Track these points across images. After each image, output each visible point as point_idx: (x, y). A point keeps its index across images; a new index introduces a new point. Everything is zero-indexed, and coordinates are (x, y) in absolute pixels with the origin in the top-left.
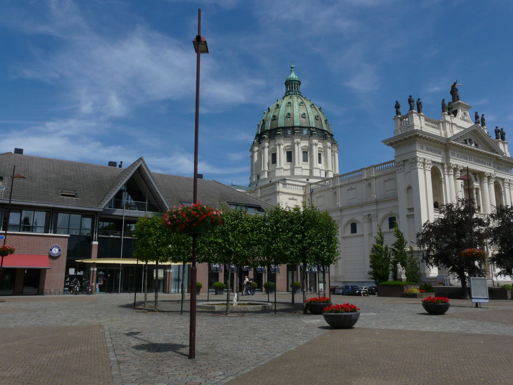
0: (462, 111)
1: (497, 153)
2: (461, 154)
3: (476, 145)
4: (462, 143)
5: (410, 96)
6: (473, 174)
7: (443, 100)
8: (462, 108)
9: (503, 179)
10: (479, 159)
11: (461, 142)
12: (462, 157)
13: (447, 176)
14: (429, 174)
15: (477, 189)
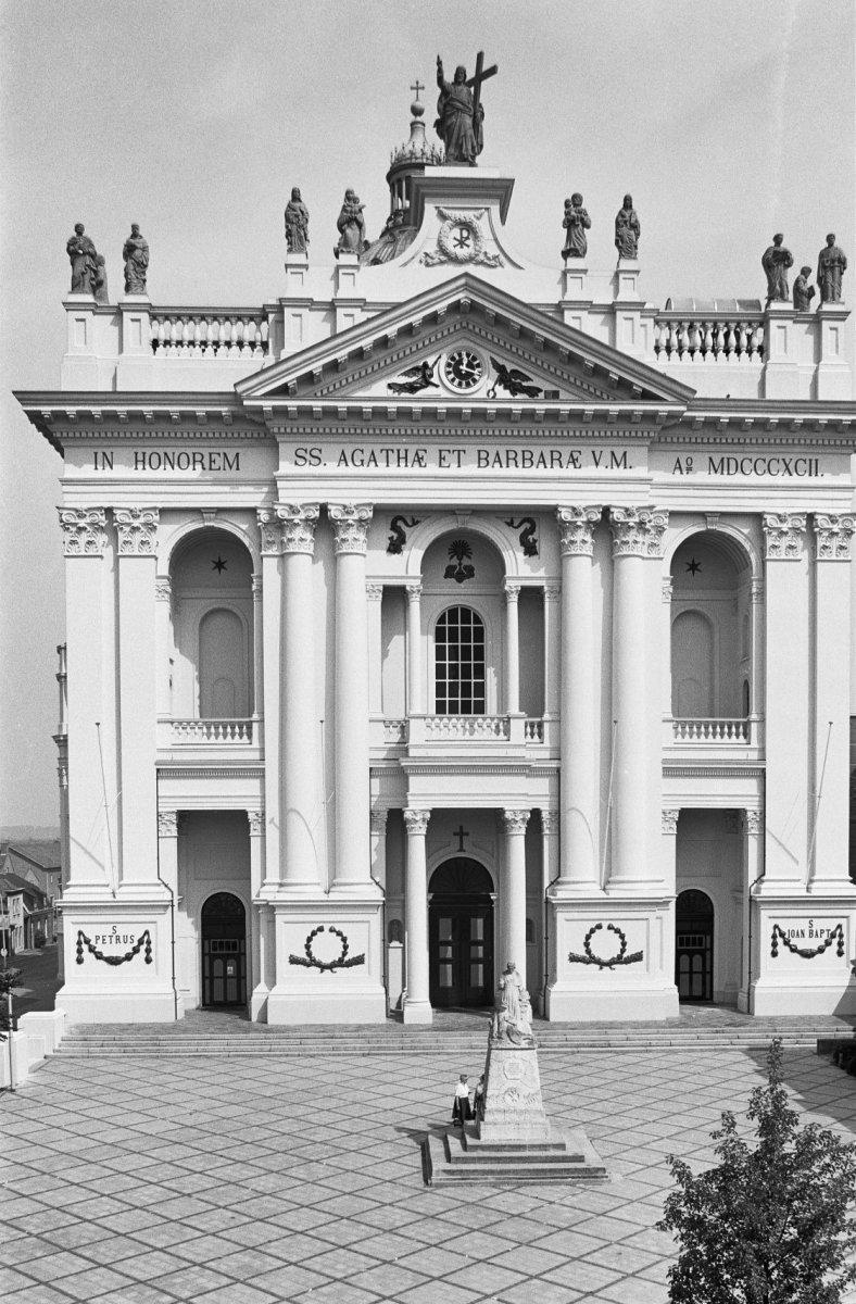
0: (443, 217)
1: (647, 396)
2: (368, 449)
3: (508, 379)
4: (390, 386)
5: (79, 229)
6: (510, 524)
7: (296, 196)
8: (443, 204)
9: (758, 517)
10: (519, 449)
11: (380, 389)
12: (380, 457)
13: (269, 569)
14: (147, 575)
15: (531, 598)
